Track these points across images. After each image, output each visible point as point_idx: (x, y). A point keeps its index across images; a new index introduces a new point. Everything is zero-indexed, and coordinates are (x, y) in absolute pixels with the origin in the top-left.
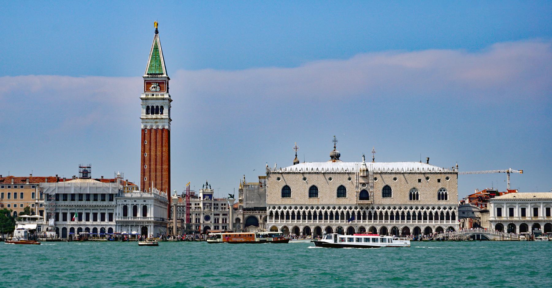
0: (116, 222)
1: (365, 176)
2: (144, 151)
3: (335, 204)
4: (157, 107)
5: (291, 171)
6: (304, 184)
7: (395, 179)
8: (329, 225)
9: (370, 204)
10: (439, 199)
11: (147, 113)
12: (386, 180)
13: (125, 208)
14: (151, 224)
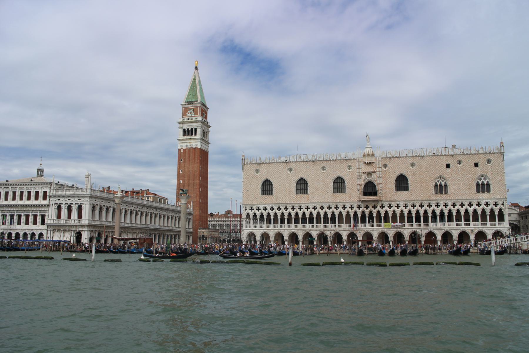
0: (48, 226)
1: (370, 163)
2: (180, 168)
3: (329, 203)
4: (192, 129)
5: (273, 161)
6: (289, 176)
7: (413, 165)
8: (322, 230)
9: (377, 200)
10: (478, 191)
11: (184, 135)
12: (400, 167)
13: (59, 208)
14: (85, 229)
